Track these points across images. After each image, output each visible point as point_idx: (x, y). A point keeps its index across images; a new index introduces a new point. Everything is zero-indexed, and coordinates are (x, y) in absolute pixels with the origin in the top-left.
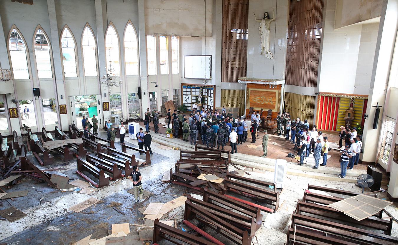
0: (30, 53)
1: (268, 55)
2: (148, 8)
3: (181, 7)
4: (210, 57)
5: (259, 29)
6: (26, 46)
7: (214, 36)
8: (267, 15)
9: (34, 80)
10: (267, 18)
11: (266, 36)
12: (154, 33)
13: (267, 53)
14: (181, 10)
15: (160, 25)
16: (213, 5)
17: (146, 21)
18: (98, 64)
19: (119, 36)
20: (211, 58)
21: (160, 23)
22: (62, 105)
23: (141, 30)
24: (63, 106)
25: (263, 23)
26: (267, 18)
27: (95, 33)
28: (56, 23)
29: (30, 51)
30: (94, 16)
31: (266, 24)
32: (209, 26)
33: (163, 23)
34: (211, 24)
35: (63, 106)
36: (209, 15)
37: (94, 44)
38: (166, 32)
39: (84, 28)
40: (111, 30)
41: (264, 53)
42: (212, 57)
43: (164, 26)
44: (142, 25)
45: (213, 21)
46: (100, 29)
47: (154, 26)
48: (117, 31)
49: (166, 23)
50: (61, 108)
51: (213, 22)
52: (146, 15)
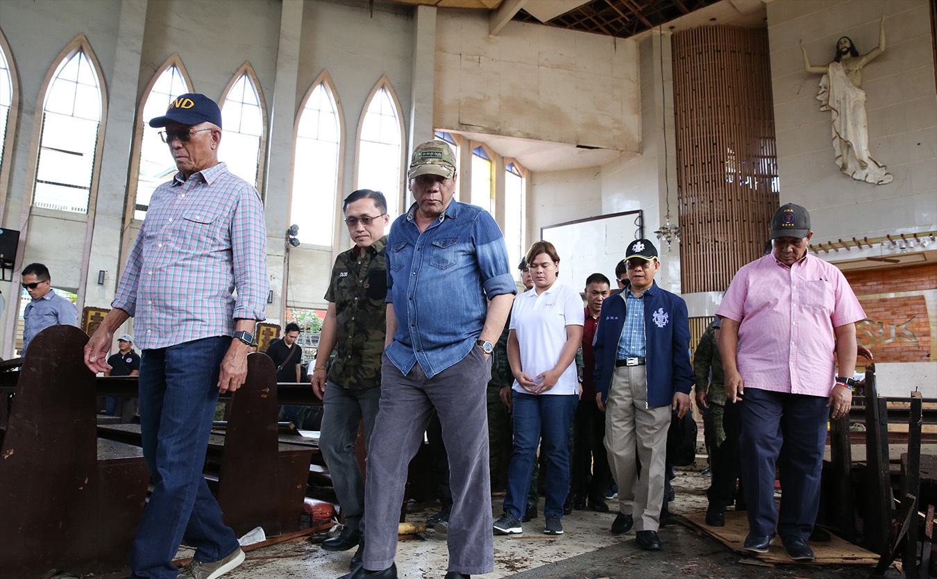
0: (25, 116)
1: (867, 171)
2: (445, 52)
3: (547, 60)
4: (638, 215)
5: (818, 98)
6: (17, 87)
7: (653, 150)
8: (848, 45)
9: (12, 207)
10: (849, 54)
11: (854, 107)
12: (459, 123)
13: (863, 165)
14: (547, 67)
15: (480, 101)
16: (640, 63)
17: (438, 85)
18: (265, 172)
19: (345, 129)
20: (641, 217)
21: (480, 97)
22: (95, 309)
23: (418, 101)
24: (98, 315)
25: (836, 73)
26: (849, 54)
27: (266, 96)
28: (140, 29)
29: (25, 107)
30: (274, 50)
31: (848, 72)
32: (632, 123)
33: (489, 97)
34: (636, 115)
35: (98, 315)
36: (630, 89)
37: (259, 129)
38: (498, 124)
39: (234, 74)
40: (321, 100)
41: (851, 167)
42: (646, 216)
43: (493, 107)
44: (422, 86)
45: (643, 108)
46: (287, 78)
47: (460, 103)
48: (338, 102)
49: (498, 100)
50: (89, 321)
51: (642, 110)
52: (439, 68)
